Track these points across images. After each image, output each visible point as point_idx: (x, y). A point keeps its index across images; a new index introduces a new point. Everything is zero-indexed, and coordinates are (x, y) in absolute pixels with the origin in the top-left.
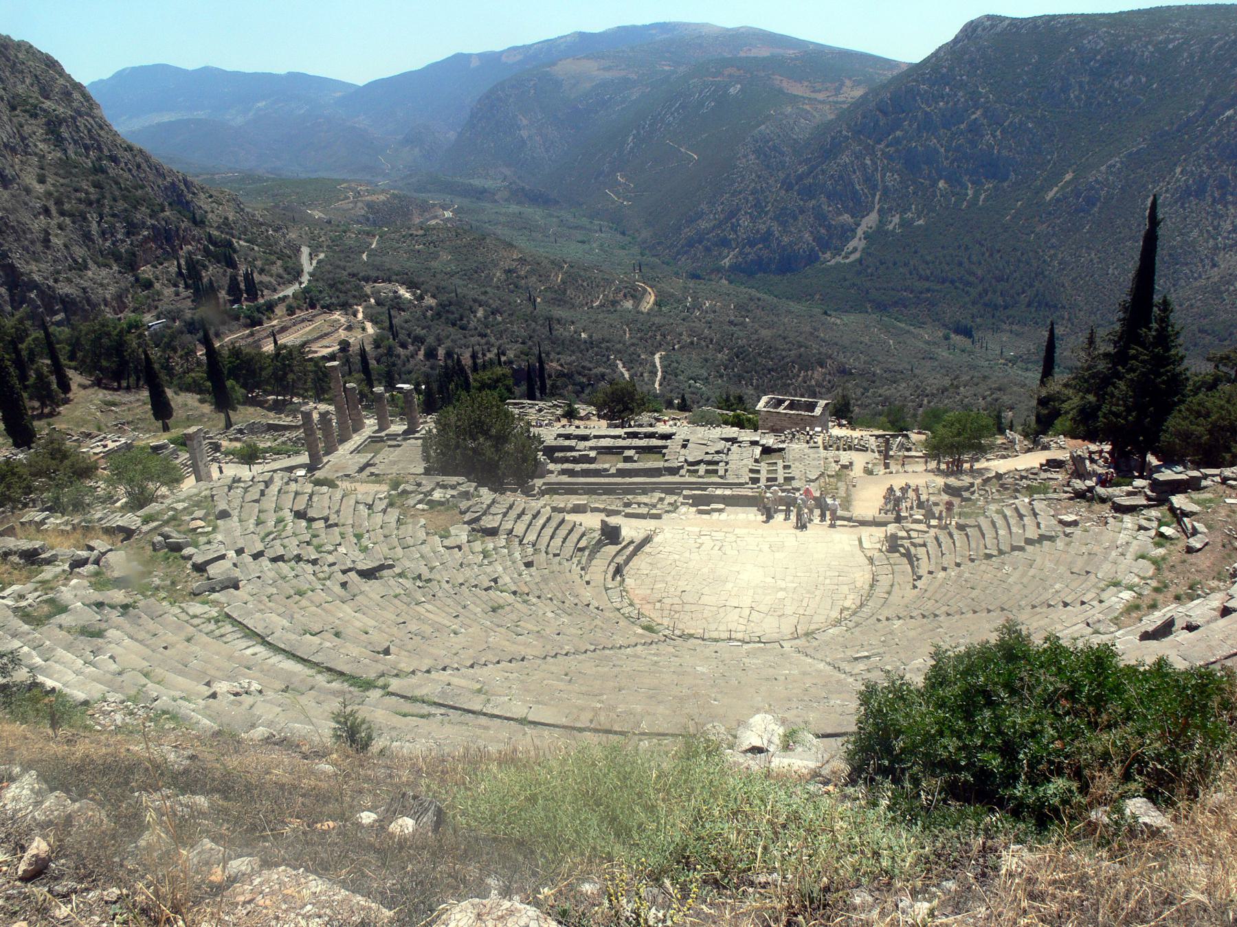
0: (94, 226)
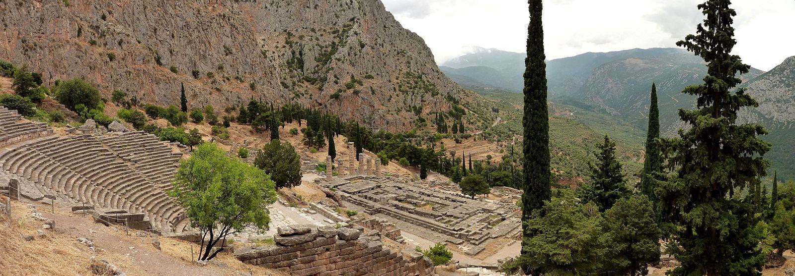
0: (410, 96)
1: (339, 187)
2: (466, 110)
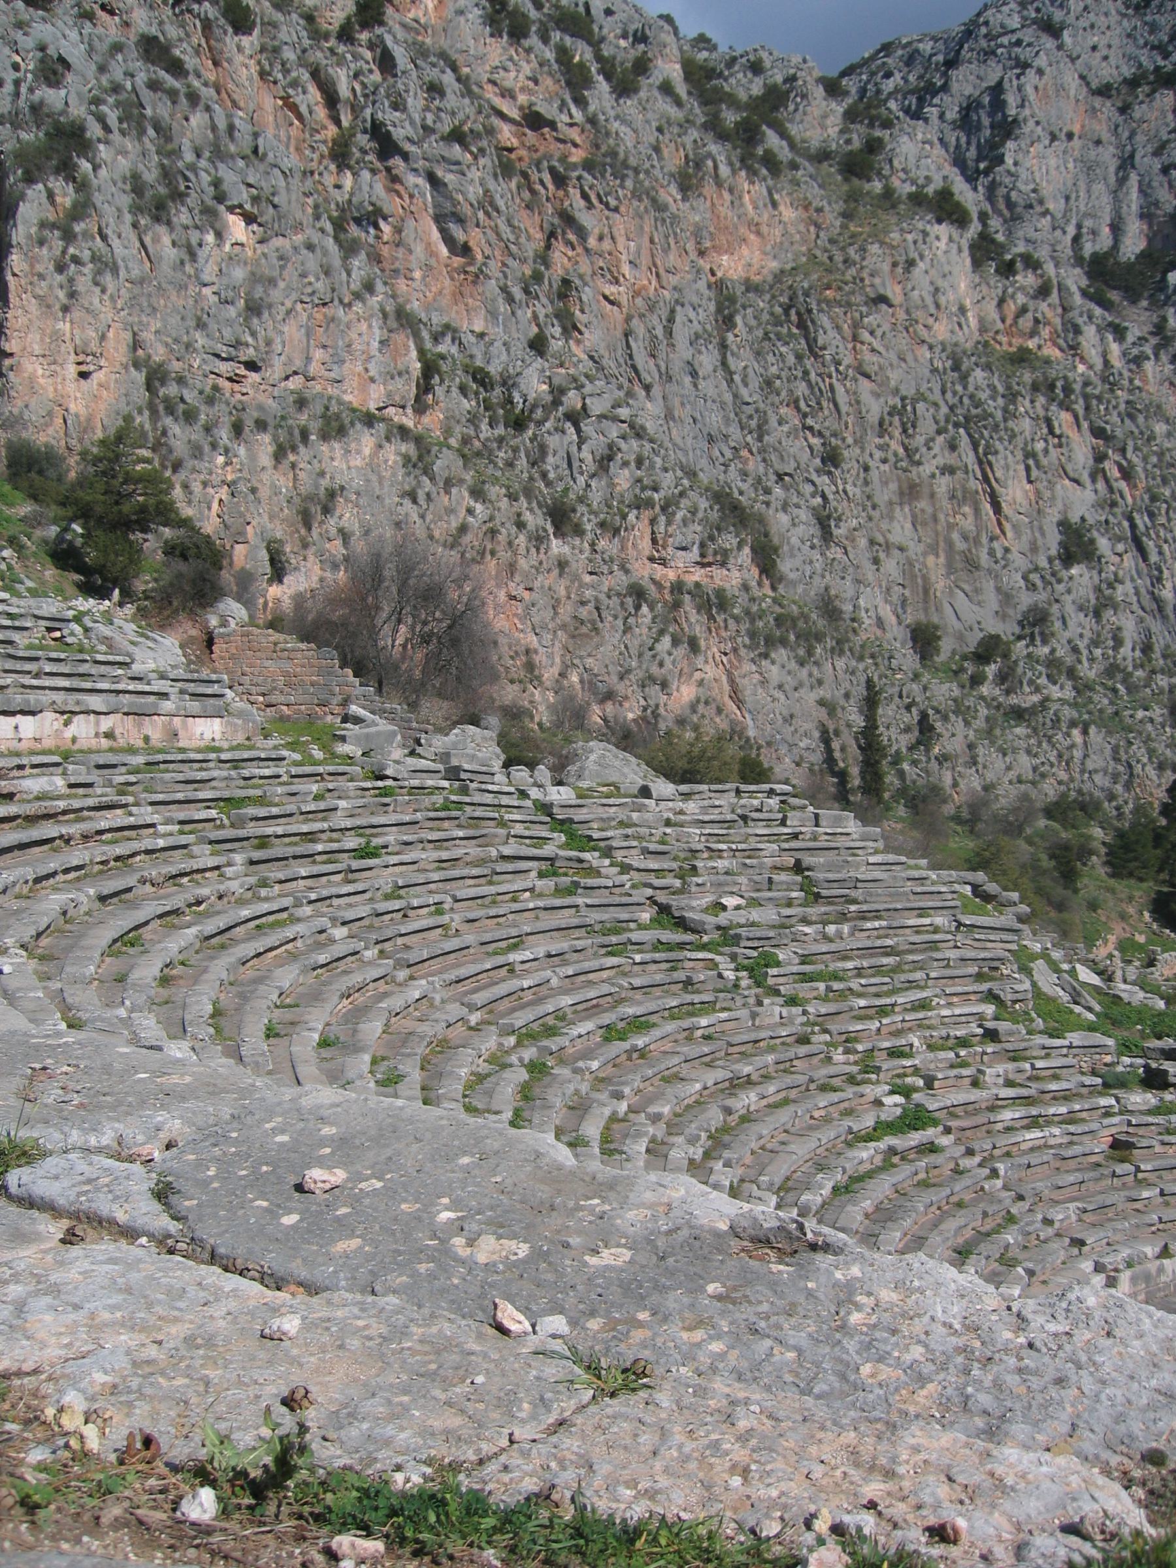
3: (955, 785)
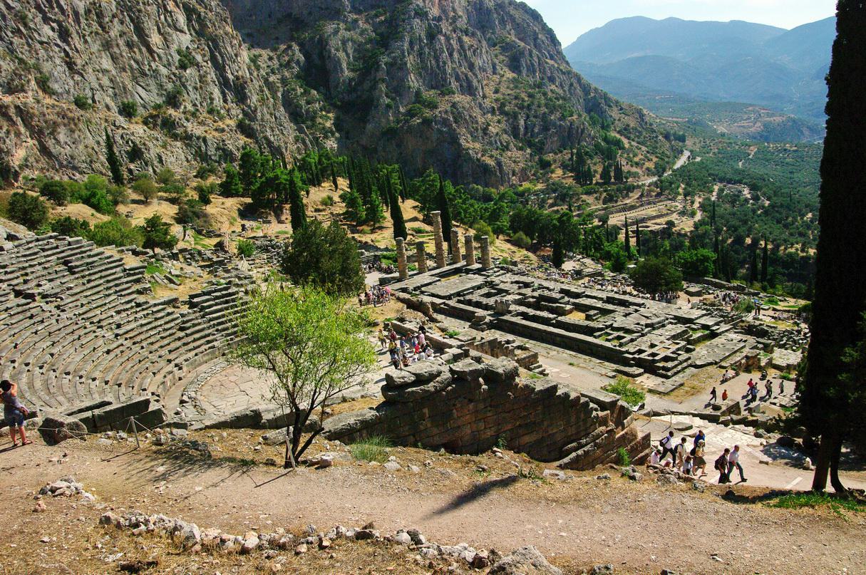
0: (522, 122)
1: (423, 289)
2: (625, 141)
3: (154, 171)
